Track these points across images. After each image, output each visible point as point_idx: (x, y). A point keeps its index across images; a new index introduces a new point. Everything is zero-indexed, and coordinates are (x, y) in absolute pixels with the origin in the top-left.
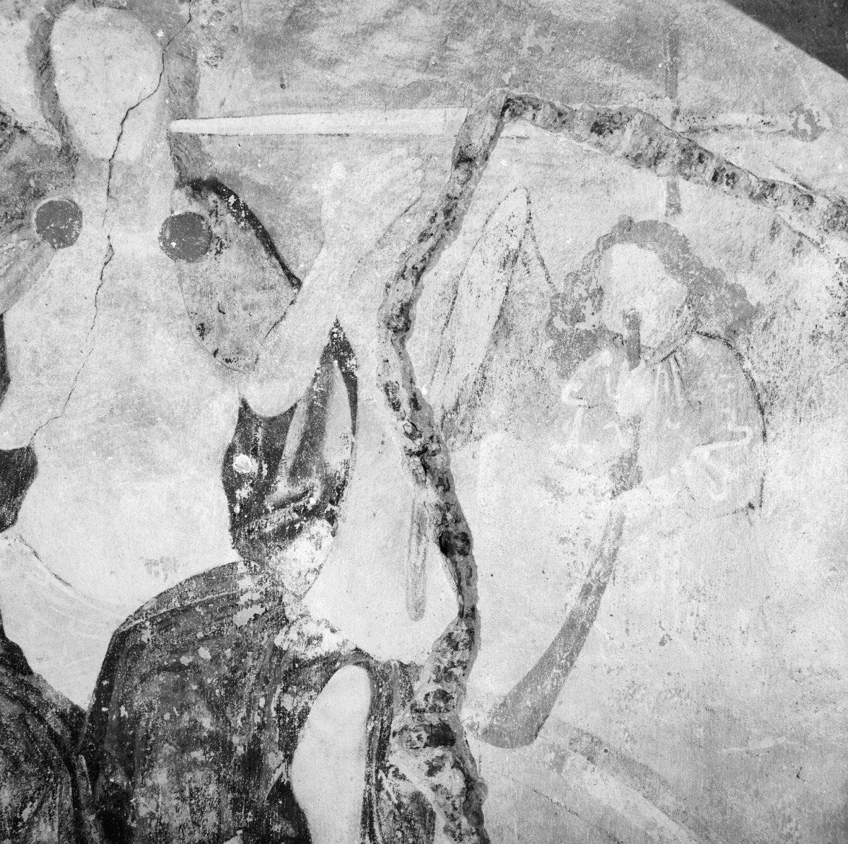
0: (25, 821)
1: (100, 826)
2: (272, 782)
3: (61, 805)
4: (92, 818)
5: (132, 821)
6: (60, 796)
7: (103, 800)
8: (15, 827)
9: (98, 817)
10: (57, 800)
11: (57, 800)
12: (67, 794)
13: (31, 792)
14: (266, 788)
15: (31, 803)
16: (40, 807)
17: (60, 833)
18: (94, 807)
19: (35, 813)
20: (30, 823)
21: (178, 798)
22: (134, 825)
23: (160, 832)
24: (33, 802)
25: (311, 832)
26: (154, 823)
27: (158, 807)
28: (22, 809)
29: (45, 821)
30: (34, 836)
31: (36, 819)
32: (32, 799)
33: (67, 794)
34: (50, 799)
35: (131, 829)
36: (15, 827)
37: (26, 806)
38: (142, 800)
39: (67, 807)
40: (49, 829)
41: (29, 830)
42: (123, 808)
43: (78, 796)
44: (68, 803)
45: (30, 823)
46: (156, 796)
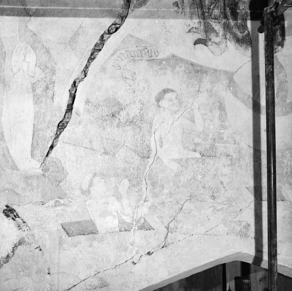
0: (211, 9)
1: (230, 11)
2: (274, 2)
3: (221, 5)
4: (228, 9)
5: (238, 10)
6: (220, 3)
7: (231, 4)
8: (209, 10)
9: (230, 9)
10: (220, 4)
11: (220, 4)
12: (222, 2)
13: (213, 1)
14: (273, 3)
15: (213, 4)
16: (215, 5)
17: (220, 12)
18: (229, 6)
19: (214, 7)
20: (213, 9)
22: (239, 11)
23: (245, 14)
24: (214, 4)
25: (284, 15)
26: (244, 11)
27: (245, 7)
28: (211, 6)
29: (216, 9)
30: (214, 13)
31: (214, 9)
32: (213, 3)
33: (222, 2)
34: (218, 4)
35: (238, 12)
36: (209, 10)
37: (212, 5)
38: (241, 5)
39: (222, 6)
40: (217, 11)
41: (212, 11)
42: (236, 7)
43: (225, 3)
44: (222, 5)
45: (213, 9)
46: (244, 4)
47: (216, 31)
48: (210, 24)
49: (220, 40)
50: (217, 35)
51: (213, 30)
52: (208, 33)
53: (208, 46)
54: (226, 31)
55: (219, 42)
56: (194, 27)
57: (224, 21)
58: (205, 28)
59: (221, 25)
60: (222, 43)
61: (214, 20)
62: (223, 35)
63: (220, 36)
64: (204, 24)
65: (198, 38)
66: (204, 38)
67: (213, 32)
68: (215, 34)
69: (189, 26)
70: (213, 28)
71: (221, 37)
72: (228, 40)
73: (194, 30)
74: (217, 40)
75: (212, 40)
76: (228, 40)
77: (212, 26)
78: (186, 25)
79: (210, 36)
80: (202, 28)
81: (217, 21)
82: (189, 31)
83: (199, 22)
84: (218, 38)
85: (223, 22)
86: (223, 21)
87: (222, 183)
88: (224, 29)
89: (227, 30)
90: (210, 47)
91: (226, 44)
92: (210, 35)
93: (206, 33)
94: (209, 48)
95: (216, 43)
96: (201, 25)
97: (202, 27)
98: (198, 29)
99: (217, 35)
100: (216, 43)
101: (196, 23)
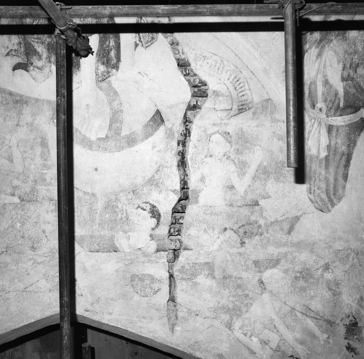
15: (36, 21)
21: (79, 21)
47: (38, 53)
48: (32, 45)
49: (44, 63)
50: (40, 58)
51: (36, 53)
52: (29, 56)
53: (29, 72)
54: (51, 53)
55: (42, 66)
56: (13, 49)
57: (48, 40)
58: (26, 50)
59: (44, 45)
60: (46, 67)
61: (36, 40)
62: (47, 58)
63: (43, 59)
64: (25, 45)
65: (17, 62)
66: (24, 62)
67: (35, 55)
68: (37, 57)
69: (8, 48)
70: (35, 50)
71: (44, 60)
72: (52, 63)
73: (14, 53)
74: (40, 64)
75: (34, 64)
76: (52, 63)
77: (33, 47)
78: (4, 47)
79: (31, 60)
80: (23, 50)
81: (40, 41)
82: (8, 54)
83: (18, 43)
84: (41, 61)
85: (47, 43)
86: (47, 41)
87: (44, 232)
88: (48, 50)
89: (51, 52)
90: (32, 72)
91: (50, 68)
92: (32, 58)
93: (27, 56)
94: (30, 74)
95: (38, 68)
96: (22, 46)
97: (23, 49)
98: (17, 51)
99: (40, 58)
100: (38, 68)
101: (16, 44)
